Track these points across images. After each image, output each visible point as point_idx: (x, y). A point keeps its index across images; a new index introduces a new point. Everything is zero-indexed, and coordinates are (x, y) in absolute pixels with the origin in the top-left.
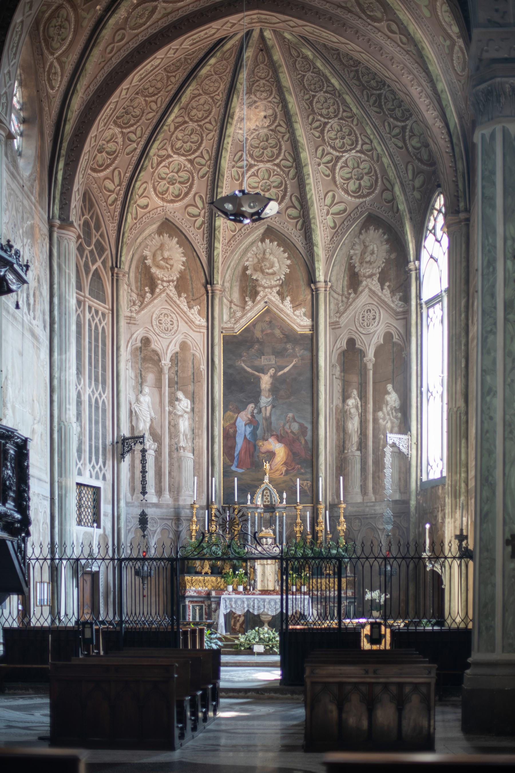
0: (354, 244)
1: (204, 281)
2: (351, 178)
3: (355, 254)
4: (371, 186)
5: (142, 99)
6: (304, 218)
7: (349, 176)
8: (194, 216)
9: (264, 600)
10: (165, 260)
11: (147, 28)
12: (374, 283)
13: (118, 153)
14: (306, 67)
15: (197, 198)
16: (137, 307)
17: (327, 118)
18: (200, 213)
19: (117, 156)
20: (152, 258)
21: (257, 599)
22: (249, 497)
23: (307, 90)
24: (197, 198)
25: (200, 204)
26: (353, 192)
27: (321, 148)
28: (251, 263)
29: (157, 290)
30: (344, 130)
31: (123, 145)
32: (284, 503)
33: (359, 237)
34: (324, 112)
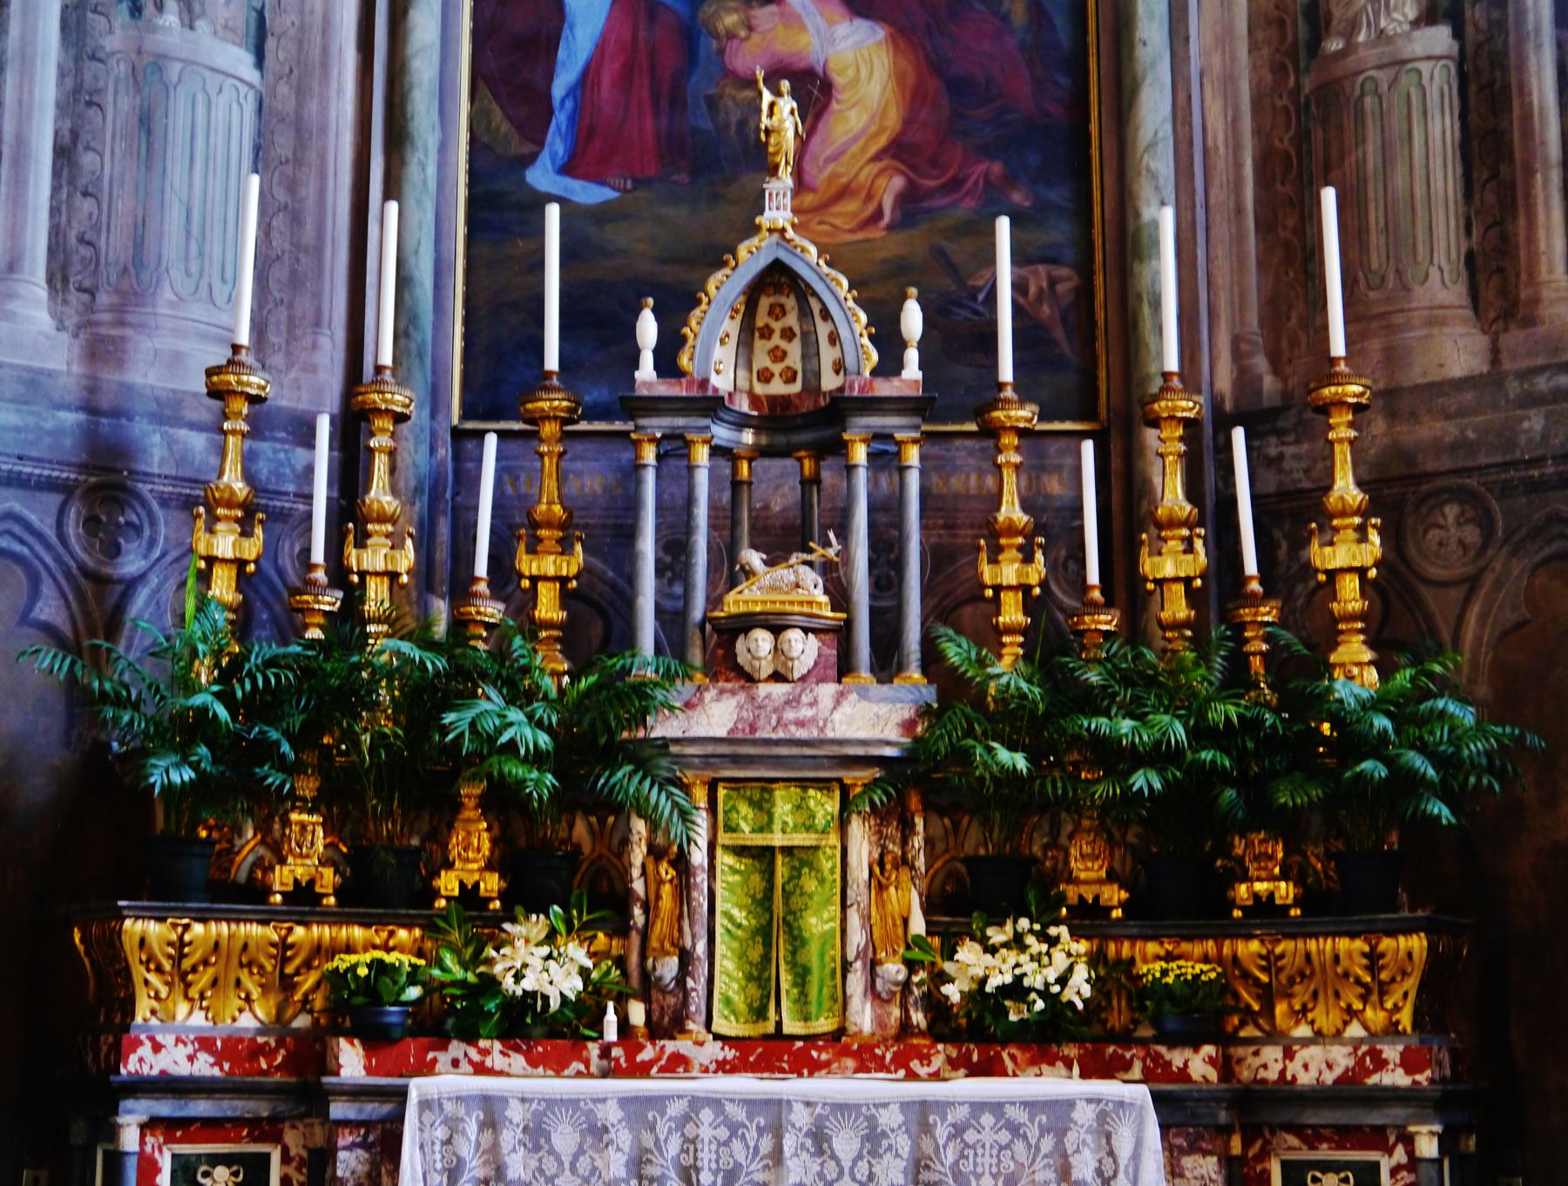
9: (773, 1113)
21: (716, 1103)
22: (648, 329)
32: (912, 369)
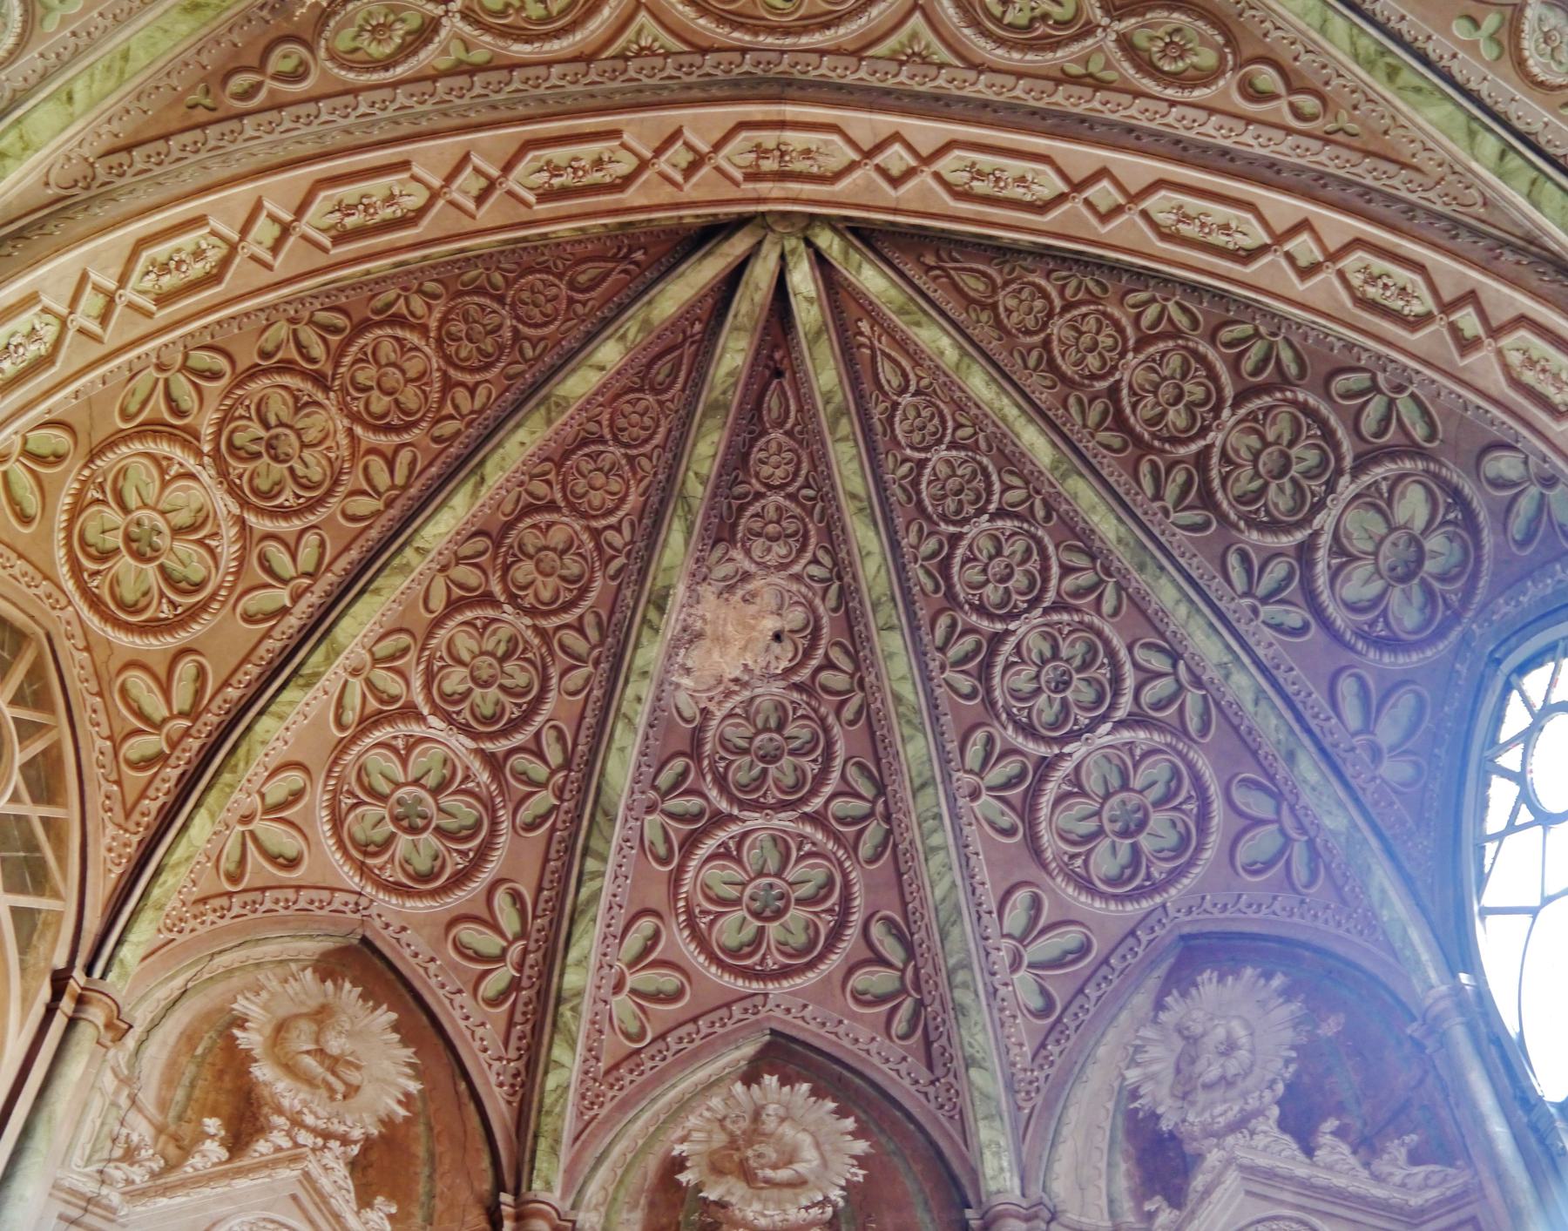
0: (1138, 1049)
1: (486, 1186)
2: (1100, 832)
3: (1151, 1077)
4: (1185, 840)
5: (342, 423)
6: (918, 989)
7: (1090, 826)
8: (479, 957)
10: (333, 1063)
11: (394, 85)
12: (1260, 1141)
13: (213, 597)
14: (931, 428)
15: (501, 899)
16: (139, 1175)
17: (1002, 618)
18: (504, 950)
19: (204, 607)
20: (268, 1030)
23: (929, 518)
24: (501, 899)
25: (509, 920)
26: (1110, 882)
27: (979, 735)
28: (698, 1147)
29: (262, 1147)
30: (1065, 652)
31: (237, 574)
33: (1155, 1021)
34: (992, 594)
